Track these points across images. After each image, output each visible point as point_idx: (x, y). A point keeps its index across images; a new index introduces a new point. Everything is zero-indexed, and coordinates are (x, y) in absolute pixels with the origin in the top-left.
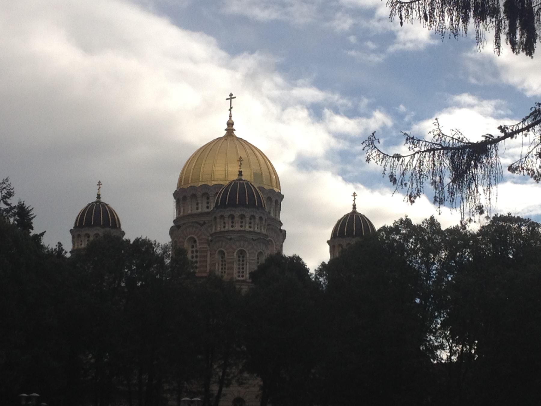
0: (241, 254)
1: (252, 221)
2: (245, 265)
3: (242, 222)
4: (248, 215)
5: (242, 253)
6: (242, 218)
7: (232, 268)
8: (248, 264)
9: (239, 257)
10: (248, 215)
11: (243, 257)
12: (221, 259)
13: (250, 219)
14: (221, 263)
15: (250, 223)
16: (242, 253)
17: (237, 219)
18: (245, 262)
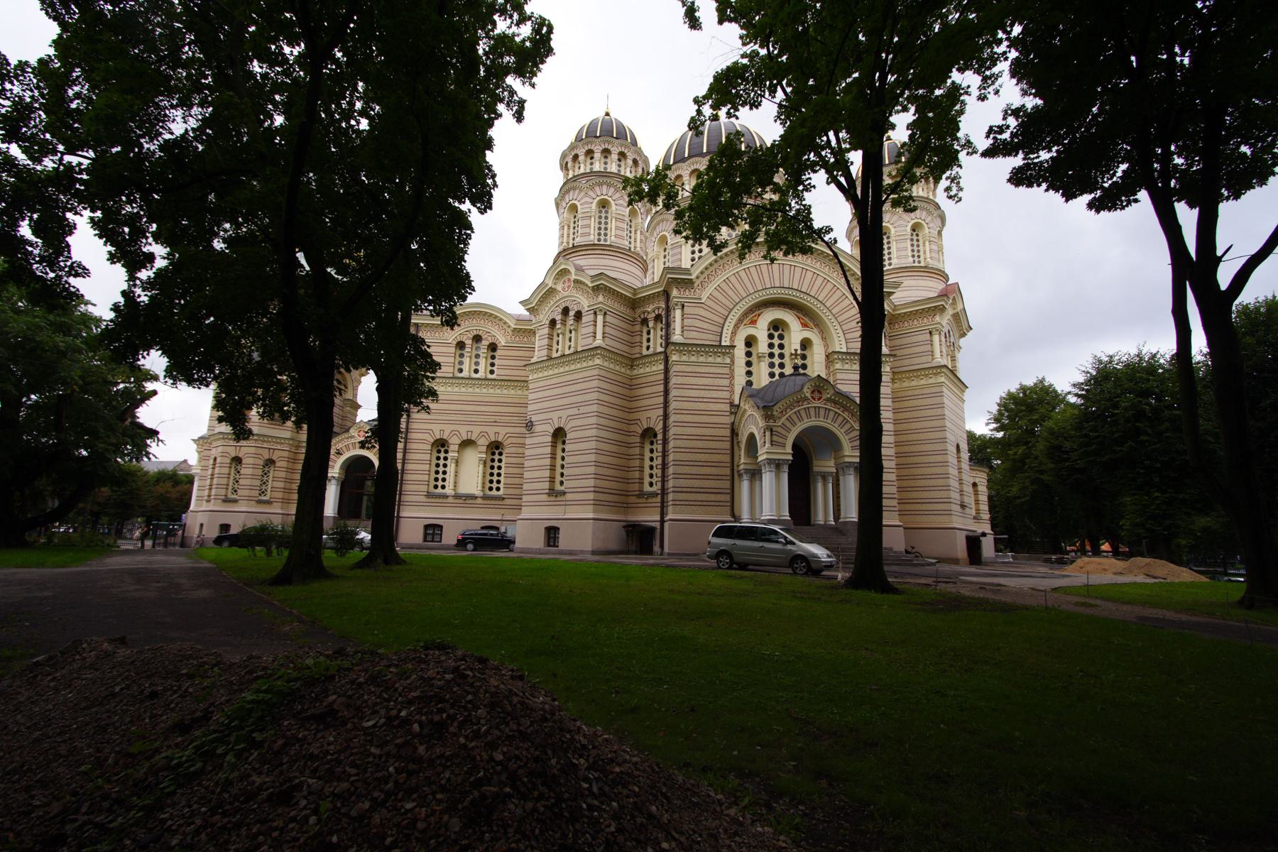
0: (604, 207)
1: (622, 163)
2: (609, 225)
3: (606, 163)
4: (615, 151)
5: (604, 205)
6: (606, 157)
7: (589, 226)
8: (614, 220)
9: (600, 212)
10: (615, 151)
11: (607, 212)
12: (573, 220)
13: (619, 160)
14: (572, 225)
15: (619, 166)
16: (604, 205)
17: (597, 155)
18: (609, 219)
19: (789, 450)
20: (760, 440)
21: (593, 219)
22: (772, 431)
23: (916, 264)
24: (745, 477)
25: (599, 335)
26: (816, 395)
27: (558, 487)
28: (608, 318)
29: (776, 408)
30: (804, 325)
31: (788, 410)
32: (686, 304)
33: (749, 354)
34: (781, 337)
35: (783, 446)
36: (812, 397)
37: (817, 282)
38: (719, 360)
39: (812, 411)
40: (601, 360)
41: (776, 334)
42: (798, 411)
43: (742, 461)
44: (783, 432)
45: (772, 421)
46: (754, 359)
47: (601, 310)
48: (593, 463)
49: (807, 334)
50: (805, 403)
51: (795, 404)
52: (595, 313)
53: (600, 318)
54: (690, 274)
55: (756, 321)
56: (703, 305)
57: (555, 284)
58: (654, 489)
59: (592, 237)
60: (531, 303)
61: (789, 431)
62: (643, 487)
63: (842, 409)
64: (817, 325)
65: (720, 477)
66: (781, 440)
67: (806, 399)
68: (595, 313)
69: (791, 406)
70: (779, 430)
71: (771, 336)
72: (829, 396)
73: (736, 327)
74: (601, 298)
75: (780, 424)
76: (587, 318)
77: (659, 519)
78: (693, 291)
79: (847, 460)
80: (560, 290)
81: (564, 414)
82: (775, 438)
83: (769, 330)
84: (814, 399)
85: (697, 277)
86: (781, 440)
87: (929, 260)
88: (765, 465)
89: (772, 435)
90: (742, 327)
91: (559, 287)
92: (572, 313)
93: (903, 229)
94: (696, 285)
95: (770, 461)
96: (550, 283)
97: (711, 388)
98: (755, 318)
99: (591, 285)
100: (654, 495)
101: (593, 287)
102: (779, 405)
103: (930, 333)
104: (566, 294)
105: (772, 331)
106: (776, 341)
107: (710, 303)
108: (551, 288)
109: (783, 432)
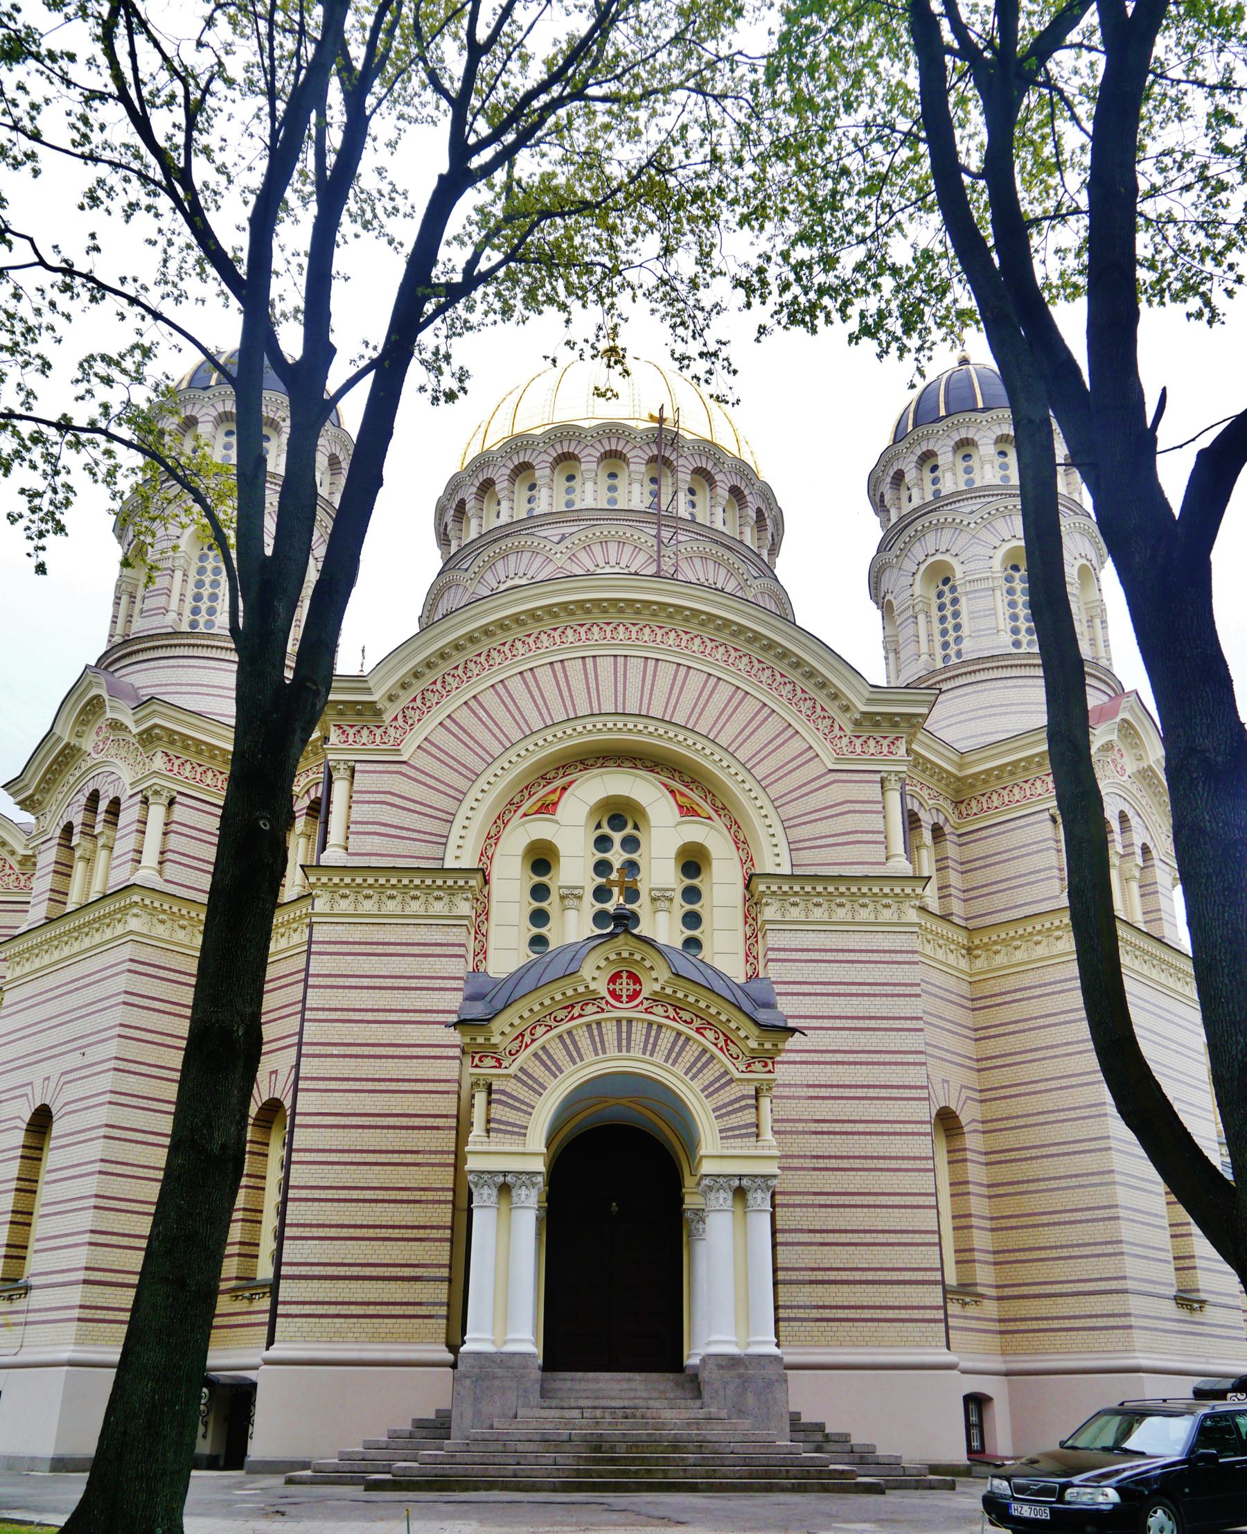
19: (537, 1140)
21: (178, 575)
22: (490, 1090)
25: (150, 857)
26: (624, 986)
28: (179, 813)
29: (498, 1025)
30: (688, 811)
31: (540, 1030)
32: (358, 767)
33: (540, 892)
34: (631, 844)
35: (521, 1131)
36: (613, 993)
37: (716, 696)
38: (438, 908)
39: (610, 1031)
40: (146, 918)
41: (617, 837)
42: (569, 1033)
44: (522, 1093)
45: (489, 1062)
46: (551, 905)
47: (156, 793)
49: (695, 832)
50: (590, 1009)
51: (561, 1015)
52: (145, 801)
53: (157, 813)
54: (368, 691)
55: (555, 804)
56: (404, 768)
57: (79, 735)
59: (172, 616)
60: (26, 787)
61: (538, 1088)
63: (697, 1023)
64: (721, 810)
65: (421, 1233)
66: (511, 1116)
67: (592, 998)
68: (145, 801)
69: (547, 1020)
70: (511, 1086)
71: (603, 843)
72: (657, 987)
73: (501, 821)
74: (159, 763)
75: (513, 1070)
76: (129, 815)
78: (379, 732)
80: (90, 750)
81: (52, 1068)
82: (498, 1111)
83: (599, 826)
84: (618, 998)
85: (392, 698)
86: (511, 1116)
89: (489, 1103)
90: (516, 819)
91: (87, 744)
92: (103, 805)
94: (387, 718)
96: (65, 734)
97: (353, 982)
98: (554, 797)
99: (135, 731)
101: (140, 734)
102: (510, 1016)
104: (99, 757)
105: (606, 830)
106: (617, 856)
107: (423, 761)
108: (68, 745)
109: (522, 1093)
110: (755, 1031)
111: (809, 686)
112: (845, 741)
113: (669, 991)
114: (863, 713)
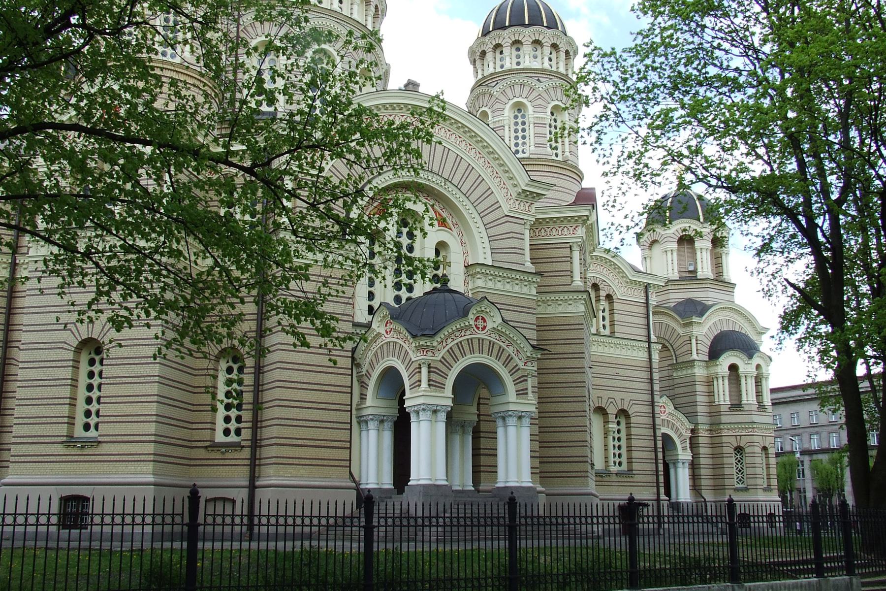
19: (448, 391)
20: (410, 377)
22: (429, 367)
23: (554, 157)
24: (372, 425)
26: (480, 323)
27: (79, 432)
31: (449, 340)
35: (442, 386)
36: (476, 326)
43: (370, 401)
44: (444, 369)
45: (430, 354)
48: (155, 398)
58: (233, 438)
62: (213, 435)
77: (247, 483)
79: (512, 407)
82: (434, 376)
84: (478, 328)
87: (567, 154)
88: (417, 412)
89: (429, 372)
93: (541, 110)
95: (425, 408)
100: (237, 446)
103: (570, 247)
109: (444, 369)
110: (531, 349)
111: (500, 170)
112: (512, 201)
113: (499, 328)
114: (524, 191)
